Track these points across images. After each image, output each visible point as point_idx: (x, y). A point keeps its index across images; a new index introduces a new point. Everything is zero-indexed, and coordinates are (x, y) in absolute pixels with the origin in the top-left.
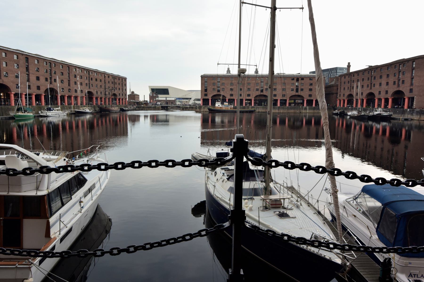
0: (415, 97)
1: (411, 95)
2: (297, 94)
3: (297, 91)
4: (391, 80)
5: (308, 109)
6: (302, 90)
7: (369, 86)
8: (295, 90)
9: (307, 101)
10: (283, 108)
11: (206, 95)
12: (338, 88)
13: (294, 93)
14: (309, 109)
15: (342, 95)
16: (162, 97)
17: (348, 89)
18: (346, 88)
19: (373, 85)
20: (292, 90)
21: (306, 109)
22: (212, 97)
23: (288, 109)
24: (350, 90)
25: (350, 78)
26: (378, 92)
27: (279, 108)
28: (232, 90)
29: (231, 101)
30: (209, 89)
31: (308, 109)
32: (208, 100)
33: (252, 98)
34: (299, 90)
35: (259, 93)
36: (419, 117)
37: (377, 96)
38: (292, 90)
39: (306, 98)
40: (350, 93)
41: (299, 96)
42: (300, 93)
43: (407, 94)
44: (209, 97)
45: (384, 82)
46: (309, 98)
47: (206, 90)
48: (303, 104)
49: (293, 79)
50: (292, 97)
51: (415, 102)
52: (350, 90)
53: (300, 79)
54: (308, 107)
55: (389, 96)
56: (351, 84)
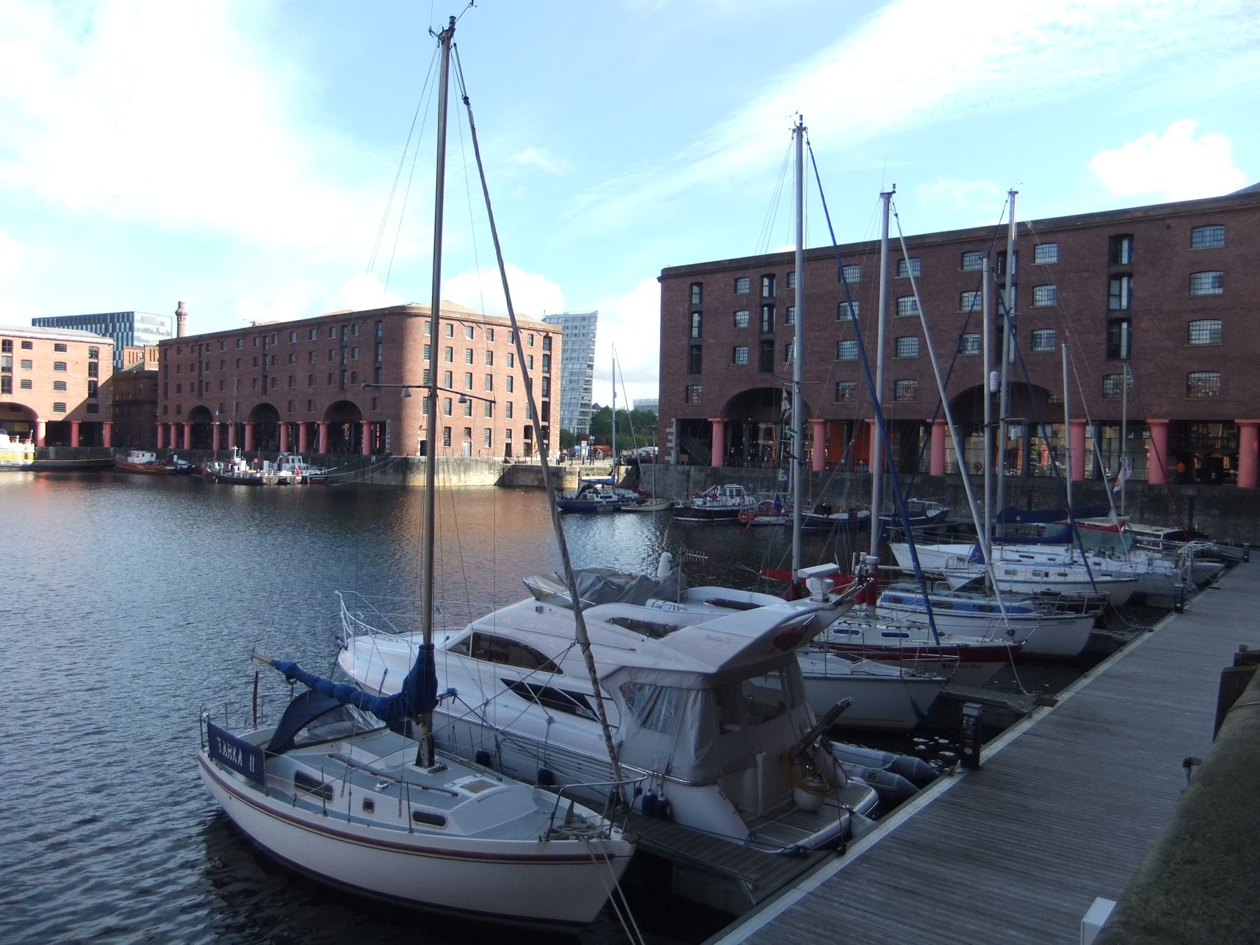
7: (260, 382)
12: (156, 385)
15: (172, 409)
17: (192, 390)
18: (186, 388)
19: (269, 380)
24: (200, 391)
25: (195, 354)
26: (286, 403)
36: (401, 477)
37: (284, 416)
39: (45, 415)
40: (200, 404)
45: (301, 376)
51: (388, 436)
52: (200, 391)
56: (200, 375)
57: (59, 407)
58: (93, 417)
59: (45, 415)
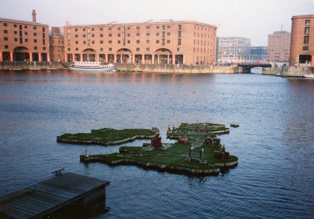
0: (184, 55)
1: (179, 53)
2: (22, 45)
3: (21, 42)
5: (35, 64)
8: (19, 39)
10: (8, 64)
14: (37, 64)
23: (14, 65)
31: (35, 64)
34: (24, 40)
38: (16, 40)
43: (175, 53)
46: (35, 51)
49: (15, 26)
53: (23, 26)
54: (35, 62)
57: (36, 48)
58: (45, 52)
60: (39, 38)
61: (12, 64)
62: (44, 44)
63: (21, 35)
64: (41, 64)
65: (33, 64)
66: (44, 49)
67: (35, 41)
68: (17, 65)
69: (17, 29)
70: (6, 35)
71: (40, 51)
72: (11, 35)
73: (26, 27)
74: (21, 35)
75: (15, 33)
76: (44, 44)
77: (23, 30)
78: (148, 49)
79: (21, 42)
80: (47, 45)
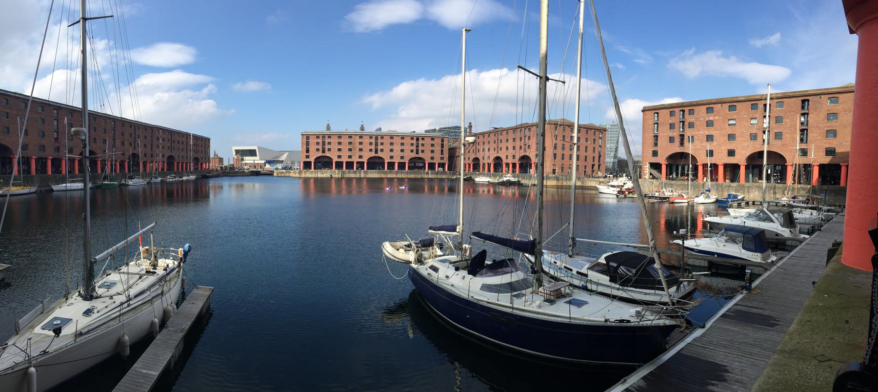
3: (417, 153)
4: (518, 144)
6: (423, 151)
9: (429, 164)
11: (307, 157)
13: (414, 155)
16: (248, 160)
20: (412, 151)
21: (428, 173)
22: (316, 159)
27: (397, 173)
28: (339, 150)
29: (339, 165)
30: (313, 148)
32: (310, 162)
33: (365, 160)
35: (373, 154)
37: (505, 161)
38: (412, 151)
39: (428, 161)
41: (420, 158)
42: (421, 155)
44: (312, 159)
45: (510, 147)
47: (308, 151)
48: (424, 167)
49: (412, 139)
50: (412, 160)
55: (516, 161)
59: (428, 161)
60: (437, 149)
61: (407, 173)
62: (442, 153)
63: (417, 146)
64: (437, 173)
65: (428, 173)
66: (442, 158)
67: (432, 151)
68: (411, 173)
69: (414, 141)
70: (403, 147)
71: (437, 161)
72: (407, 148)
73: (423, 139)
74: (417, 146)
75: (412, 144)
76: (442, 153)
77: (421, 142)
78: (514, 157)
79: (417, 153)
80: (446, 155)
